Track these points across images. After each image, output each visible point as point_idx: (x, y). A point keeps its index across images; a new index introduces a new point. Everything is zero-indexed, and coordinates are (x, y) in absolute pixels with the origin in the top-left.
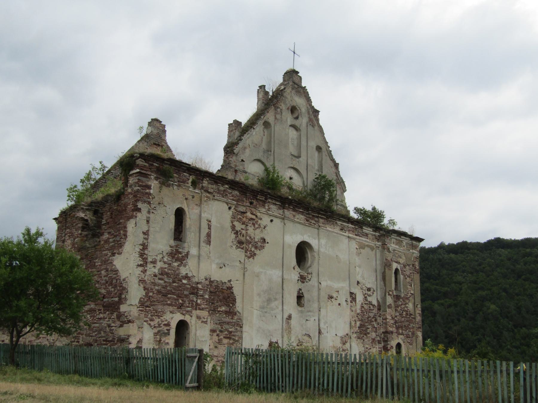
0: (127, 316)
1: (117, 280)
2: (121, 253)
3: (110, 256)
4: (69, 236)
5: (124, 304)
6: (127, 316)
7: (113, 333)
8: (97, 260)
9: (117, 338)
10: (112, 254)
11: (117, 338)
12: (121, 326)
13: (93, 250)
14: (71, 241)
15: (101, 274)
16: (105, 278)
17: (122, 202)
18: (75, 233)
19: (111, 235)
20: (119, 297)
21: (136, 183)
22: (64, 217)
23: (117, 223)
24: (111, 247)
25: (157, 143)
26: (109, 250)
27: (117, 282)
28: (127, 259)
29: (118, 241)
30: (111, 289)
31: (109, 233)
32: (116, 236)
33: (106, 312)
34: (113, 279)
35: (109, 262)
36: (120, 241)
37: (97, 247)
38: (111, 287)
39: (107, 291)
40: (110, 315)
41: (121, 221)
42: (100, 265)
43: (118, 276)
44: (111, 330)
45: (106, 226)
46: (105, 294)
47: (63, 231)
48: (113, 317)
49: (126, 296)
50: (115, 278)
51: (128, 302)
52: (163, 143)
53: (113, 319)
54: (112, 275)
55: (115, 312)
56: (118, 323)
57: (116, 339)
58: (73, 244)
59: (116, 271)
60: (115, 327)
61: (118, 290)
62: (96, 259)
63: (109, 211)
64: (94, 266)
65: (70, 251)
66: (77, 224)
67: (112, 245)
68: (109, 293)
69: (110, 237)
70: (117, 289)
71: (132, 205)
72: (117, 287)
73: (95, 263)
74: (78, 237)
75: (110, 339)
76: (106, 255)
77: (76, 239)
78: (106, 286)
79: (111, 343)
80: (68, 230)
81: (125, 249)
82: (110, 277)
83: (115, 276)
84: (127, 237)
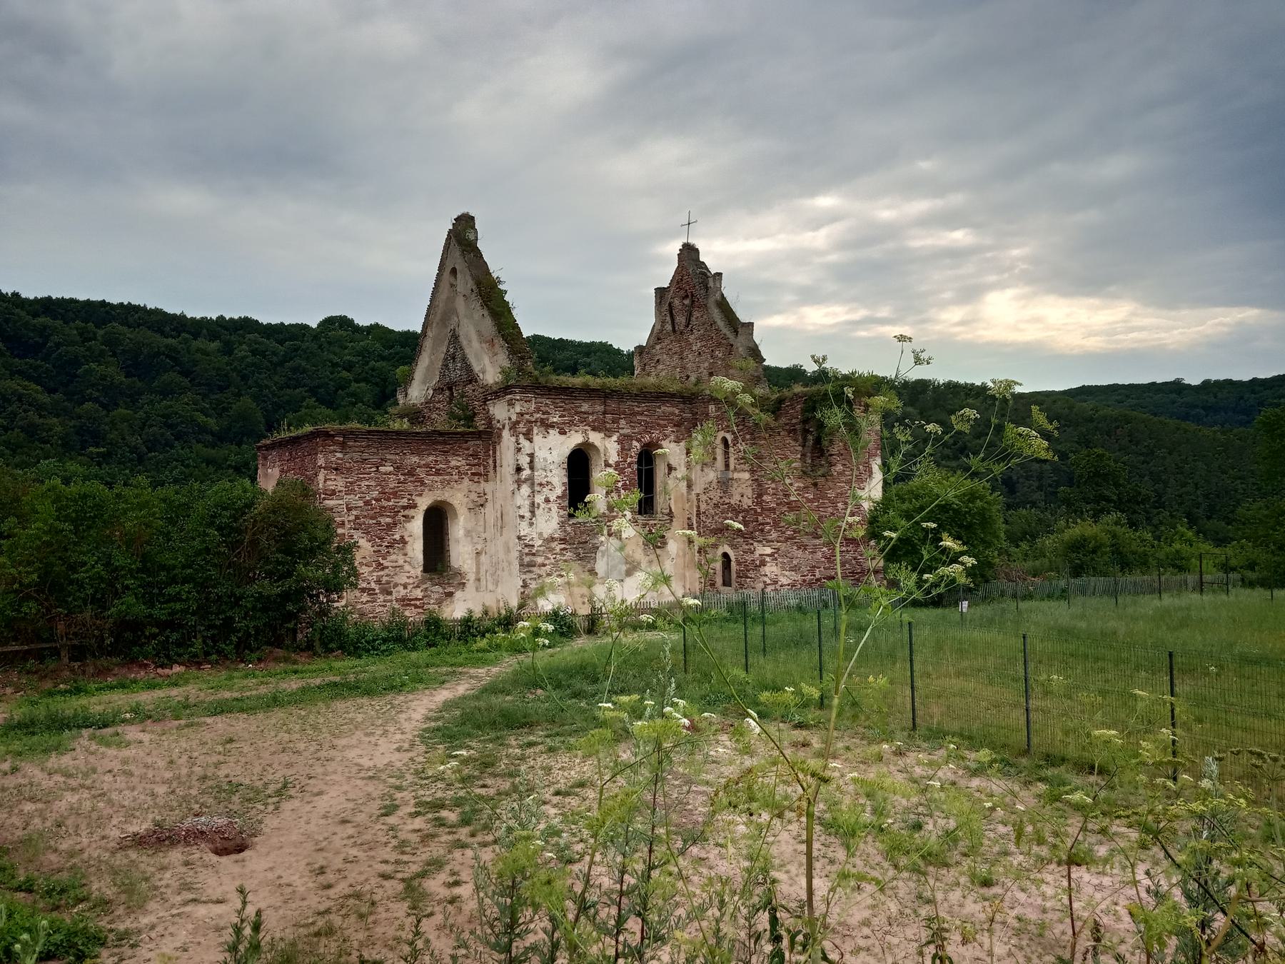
31: (844, 465)
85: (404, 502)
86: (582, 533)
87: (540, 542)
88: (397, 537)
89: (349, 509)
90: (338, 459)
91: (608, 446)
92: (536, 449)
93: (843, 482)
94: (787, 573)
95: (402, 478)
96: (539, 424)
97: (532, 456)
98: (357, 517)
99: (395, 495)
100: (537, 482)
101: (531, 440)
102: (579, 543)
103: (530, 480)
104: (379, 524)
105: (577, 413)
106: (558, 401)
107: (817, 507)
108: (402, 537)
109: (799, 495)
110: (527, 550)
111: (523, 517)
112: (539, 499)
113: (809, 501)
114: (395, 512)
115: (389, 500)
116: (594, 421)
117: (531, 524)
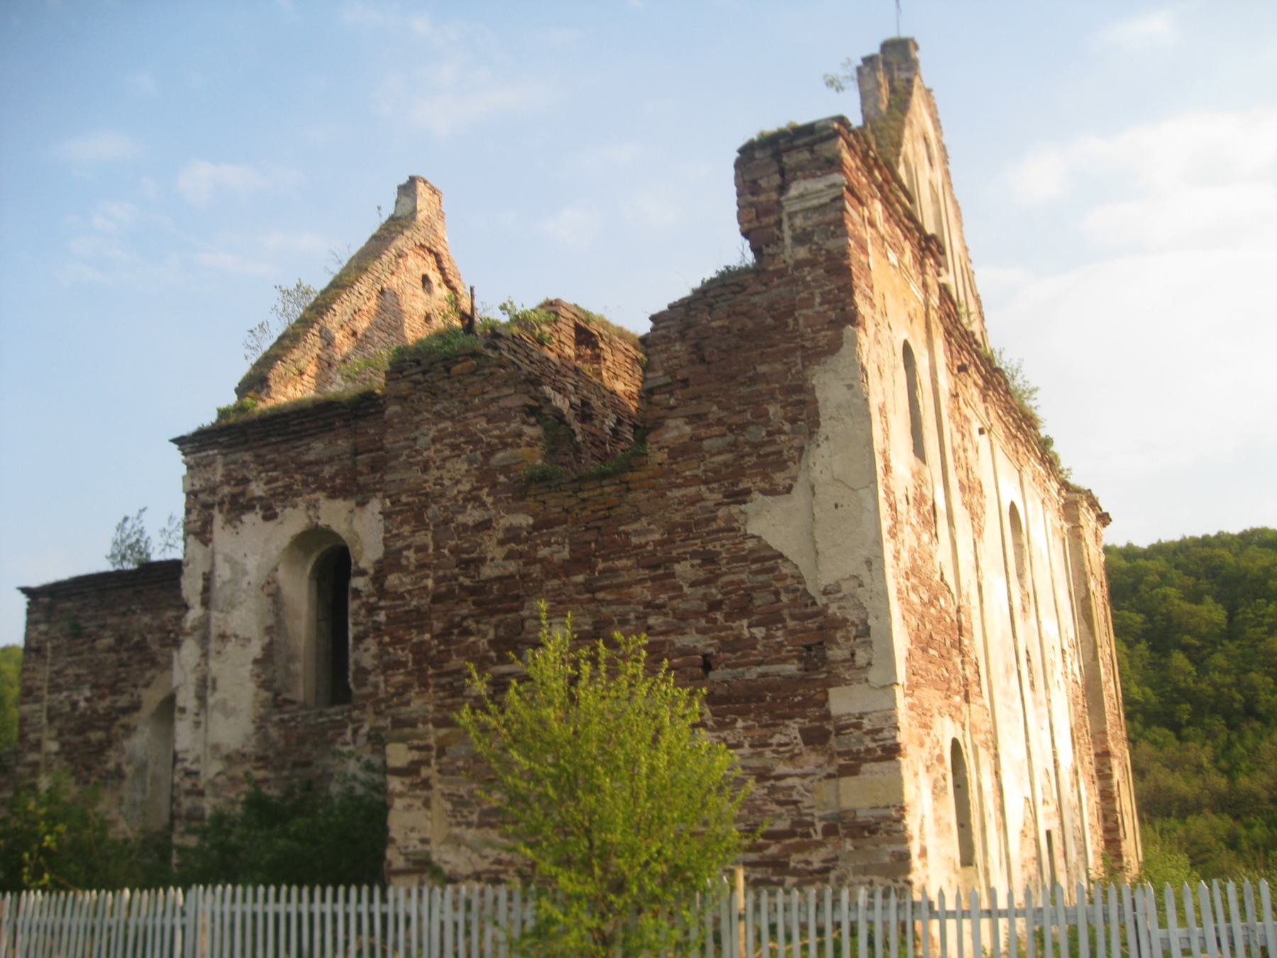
0: (881, 730)
1: (777, 594)
2: (789, 490)
3: (719, 504)
4: (454, 447)
5: (846, 682)
6: (881, 730)
7: (795, 803)
8: (635, 526)
9: (821, 819)
10: (725, 497)
11: (821, 819)
12: (849, 771)
13: (608, 489)
14: (471, 461)
15: (673, 575)
16: (701, 591)
17: (756, 299)
18: (485, 431)
19: (709, 426)
20: (800, 659)
21: (829, 224)
22: (418, 377)
23: (741, 379)
24: (716, 471)
25: (428, 245)
26: (706, 482)
27: (779, 600)
28: (836, 506)
29: (756, 446)
30: (746, 633)
31: (693, 419)
32: (743, 427)
33: (735, 721)
34: (753, 589)
35: (714, 526)
36: (775, 442)
37: (630, 476)
38: (745, 622)
39: (722, 639)
40: (758, 732)
41: (763, 369)
42: (657, 543)
43: (783, 578)
44: (772, 790)
45: (671, 394)
46: (711, 650)
47: (417, 428)
48: (778, 739)
49: (853, 655)
50: (764, 586)
51: (874, 675)
52: (440, 249)
53: (780, 745)
54: (744, 576)
55: (791, 717)
56: (811, 760)
57: (819, 826)
58: (486, 476)
59: (768, 559)
60: (804, 776)
61: (792, 632)
62: (637, 519)
63: (682, 336)
64: (624, 549)
65: (466, 500)
66: (493, 400)
67: (726, 465)
68: (736, 645)
69: (703, 432)
70: (785, 627)
71: (821, 304)
72: (783, 621)
73: (627, 534)
74: (505, 446)
75: (782, 825)
76: (693, 504)
77: (499, 455)
78: (715, 621)
79: (788, 841)
80: (442, 426)
81: (818, 468)
82: (732, 583)
83: (761, 578)
84: (818, 424)
85: (123, 701)
86: (302, 740)
87: (217, 766)
88: (111, 765)
89: (51, 719)
90: (41, 633)
91: (358, 526)
92: (219, 559)
93: (688, 483)
94: (470, 834)
95: (125, 655)
96: (226, 507)
97: (208, 578)
98: (60, 733)
99: (114, 690)
100: (214, 631)
101: (206, 542)
102: (296, 765)
103: (204, 624)
104: (87, 742)
105: (301, 467)
106: (264, 451)
107: (589, 588)
108: (119, 766)
109: (509, 556)
110: (187, 784)
111: (183, 710)
112: (214, 666)
113: (552, 570)
114: (110, 717)
115: (102, 697)
116: (332, 478)
117: (197, 724)
